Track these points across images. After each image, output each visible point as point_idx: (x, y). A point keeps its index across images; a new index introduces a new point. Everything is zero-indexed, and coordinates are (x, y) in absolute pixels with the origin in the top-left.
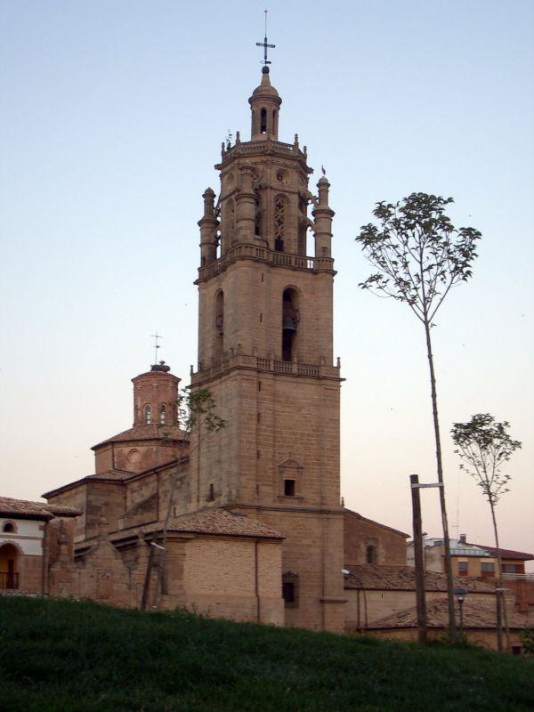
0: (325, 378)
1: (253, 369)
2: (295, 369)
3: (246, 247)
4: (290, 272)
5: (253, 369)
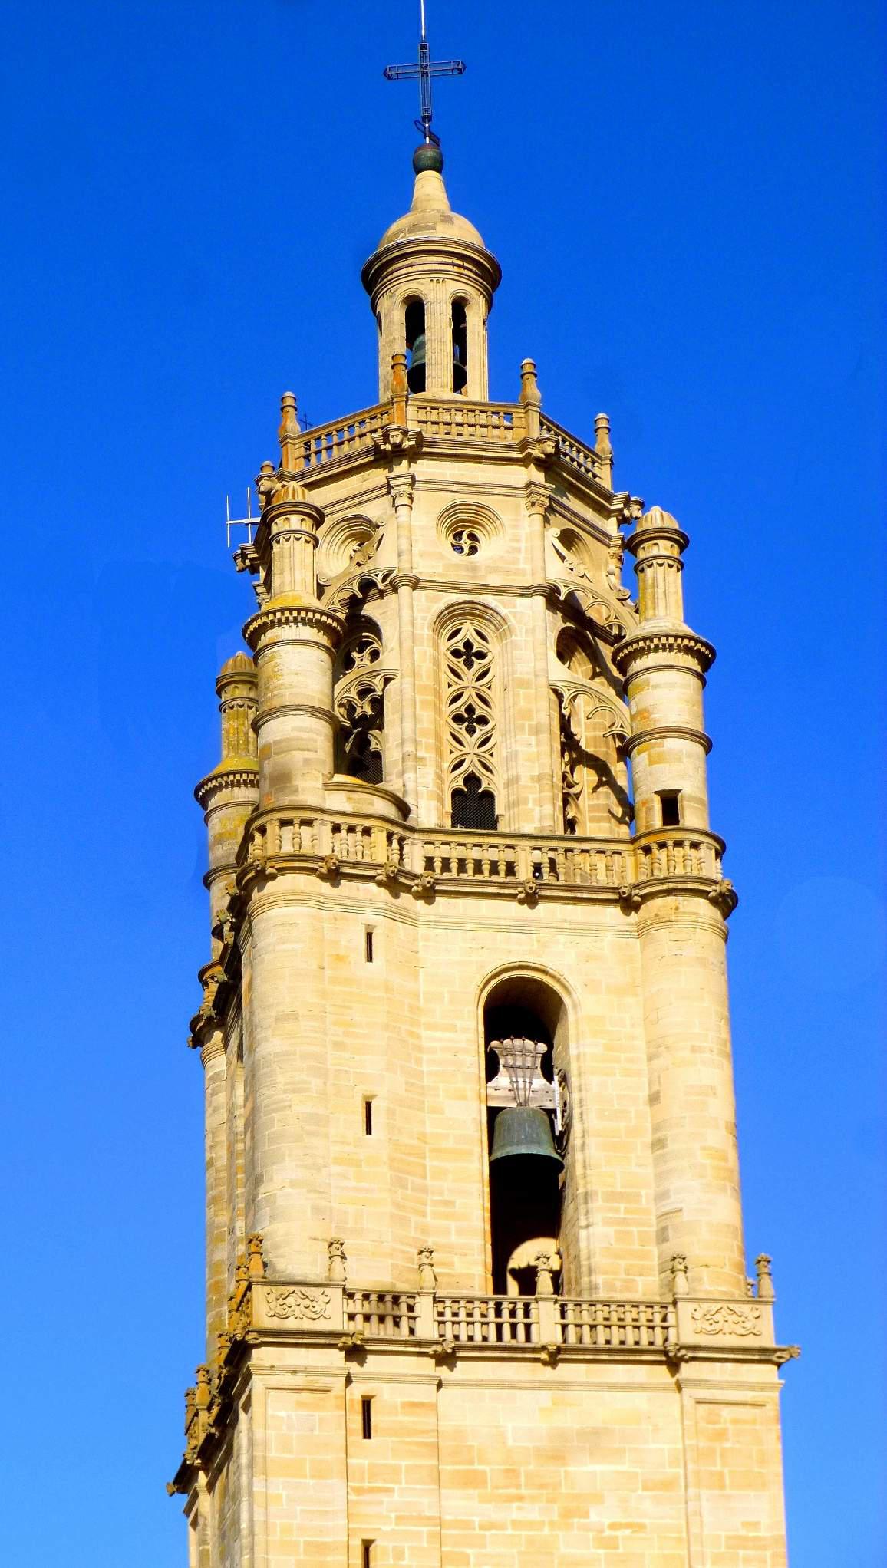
0: (695, 1353)
1: (327, 1339)
2: (546, 1327)
3: (285, 823)
4: (513, 909)
5: (327, 1339)
